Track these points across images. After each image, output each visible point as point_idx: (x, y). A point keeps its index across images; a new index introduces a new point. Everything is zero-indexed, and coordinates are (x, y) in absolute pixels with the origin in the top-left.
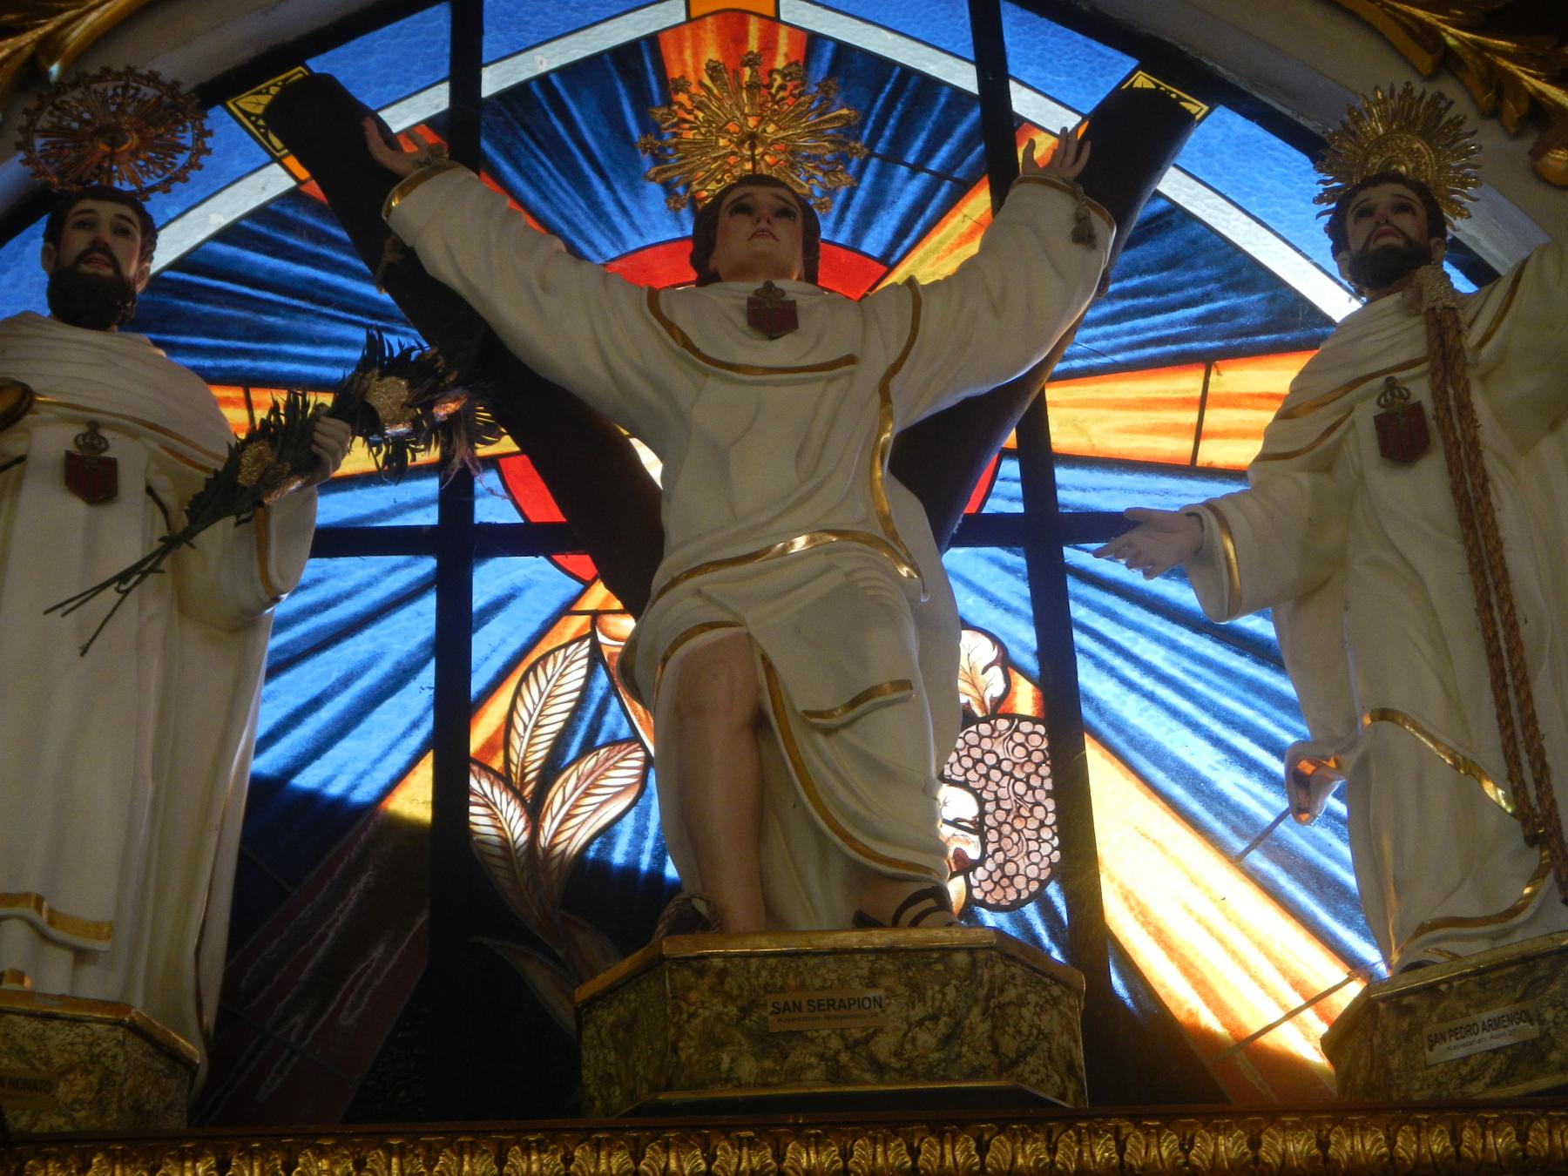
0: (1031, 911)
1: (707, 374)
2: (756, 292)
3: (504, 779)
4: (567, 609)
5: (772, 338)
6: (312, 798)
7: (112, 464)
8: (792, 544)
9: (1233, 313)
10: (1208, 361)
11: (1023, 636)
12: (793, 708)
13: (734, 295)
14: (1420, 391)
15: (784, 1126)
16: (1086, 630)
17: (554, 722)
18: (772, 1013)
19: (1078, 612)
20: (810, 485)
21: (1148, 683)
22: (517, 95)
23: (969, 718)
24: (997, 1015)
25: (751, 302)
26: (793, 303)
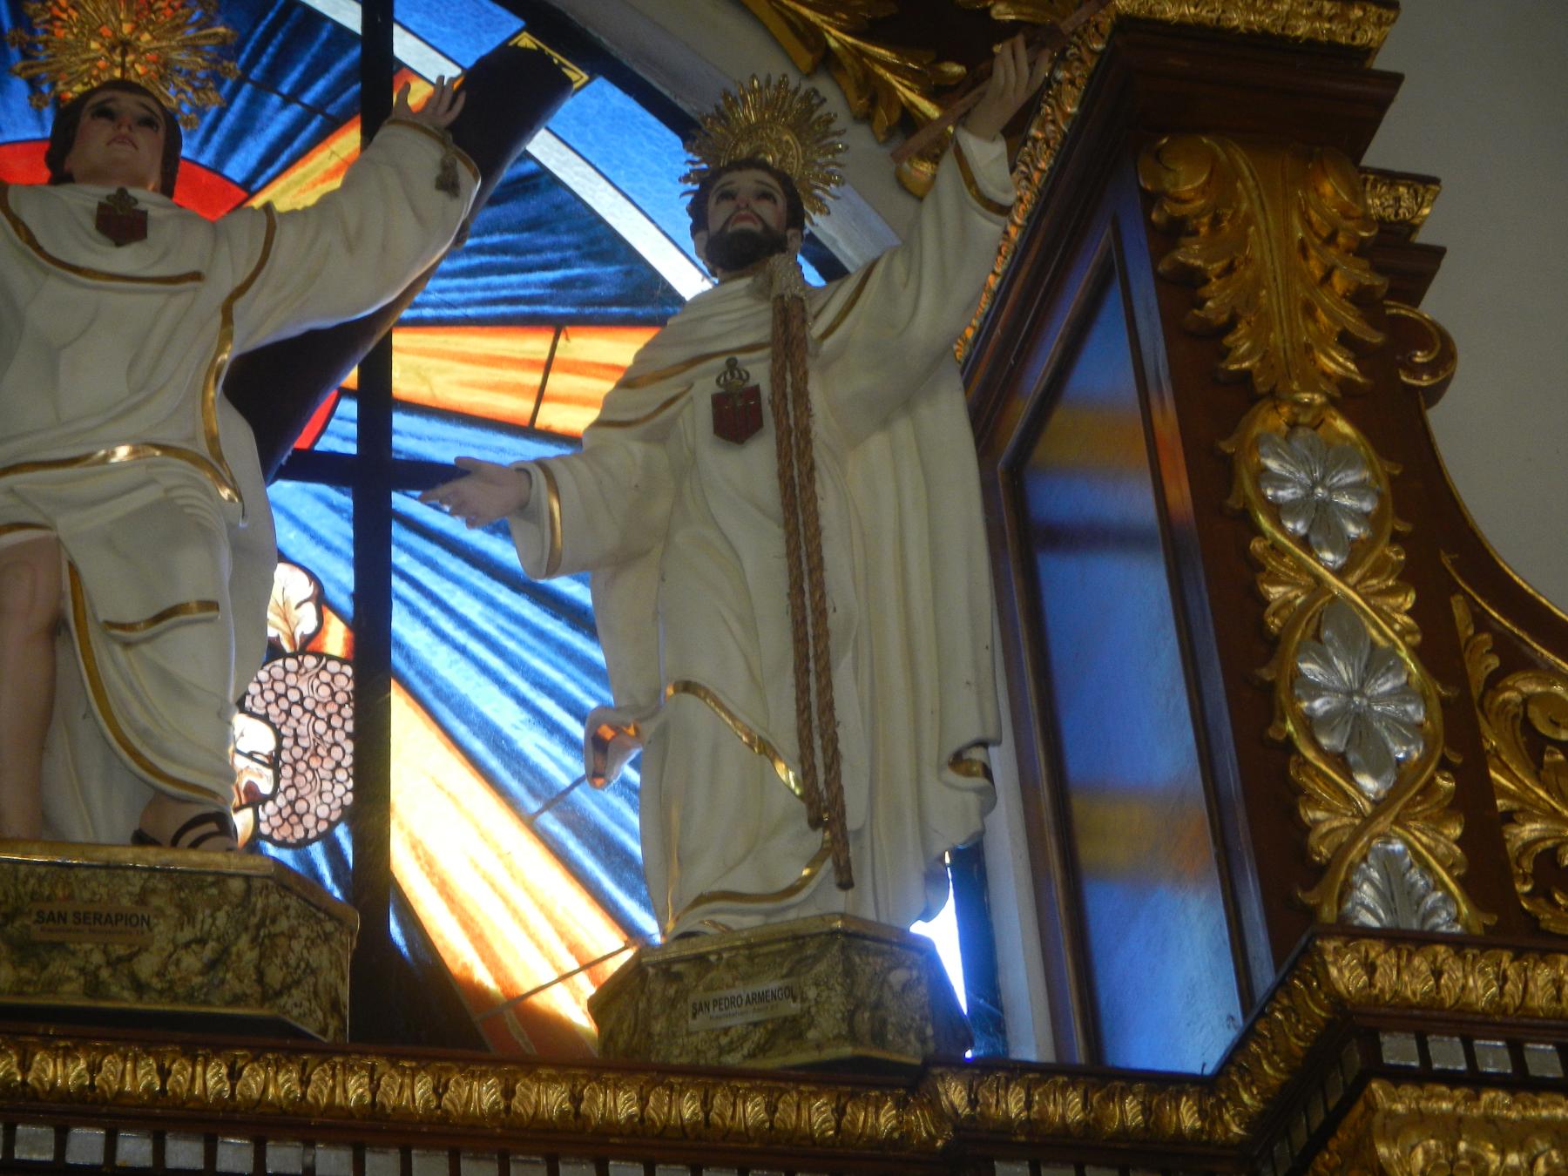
0: (317, 851)
1: (47, 272)
2: (108, 197)
5: (118, 244)
8: (113, 454)
9: (588, 282)
10: (557, 325)
11: (342, 576)
12: (95, 615)
13: (84, 198)
14: (759, 372)
15: (35, 1034)
16: (405, 577)
18: (36, 922)
19: (399, 558)
20: (142, 395)
21: (461, 637)
23: (274, 651)
24: (266, 945)
25: (101, 206)
26: (145, 213)
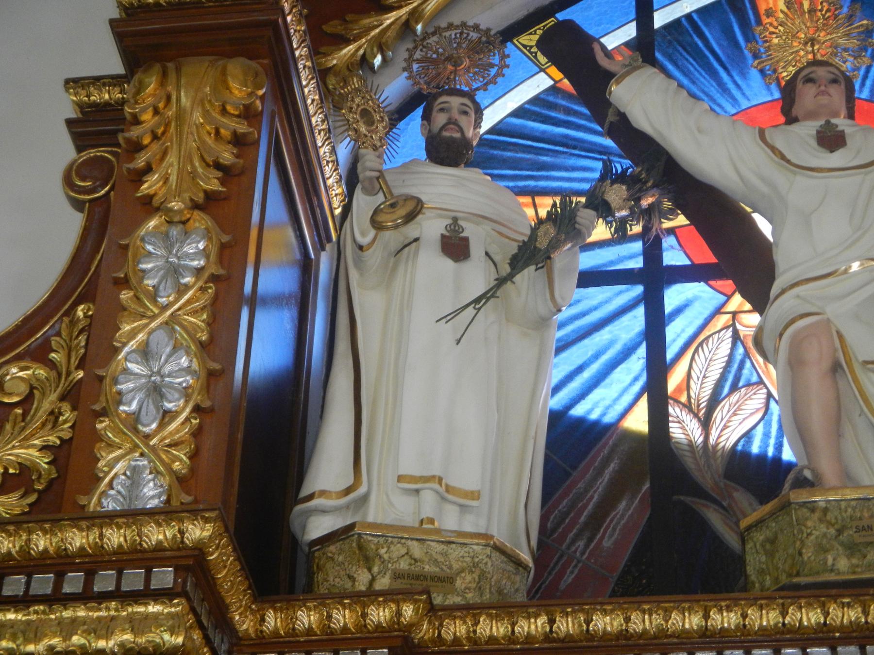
1: (795, 174)
2: (821, 126)
3: (688, 407)
4: (718, 311)
5: (832, 152)
6: (581, 421)
7: (466, 239)
8: (850, 267)
12: (857, 360)
13: (807, 129)
15: (868, 595)
17: (714, 374)
18: (856, 532)
20: (859, 233)
22: (674, 26)
25: (818, 132)
26: (843, 131)
